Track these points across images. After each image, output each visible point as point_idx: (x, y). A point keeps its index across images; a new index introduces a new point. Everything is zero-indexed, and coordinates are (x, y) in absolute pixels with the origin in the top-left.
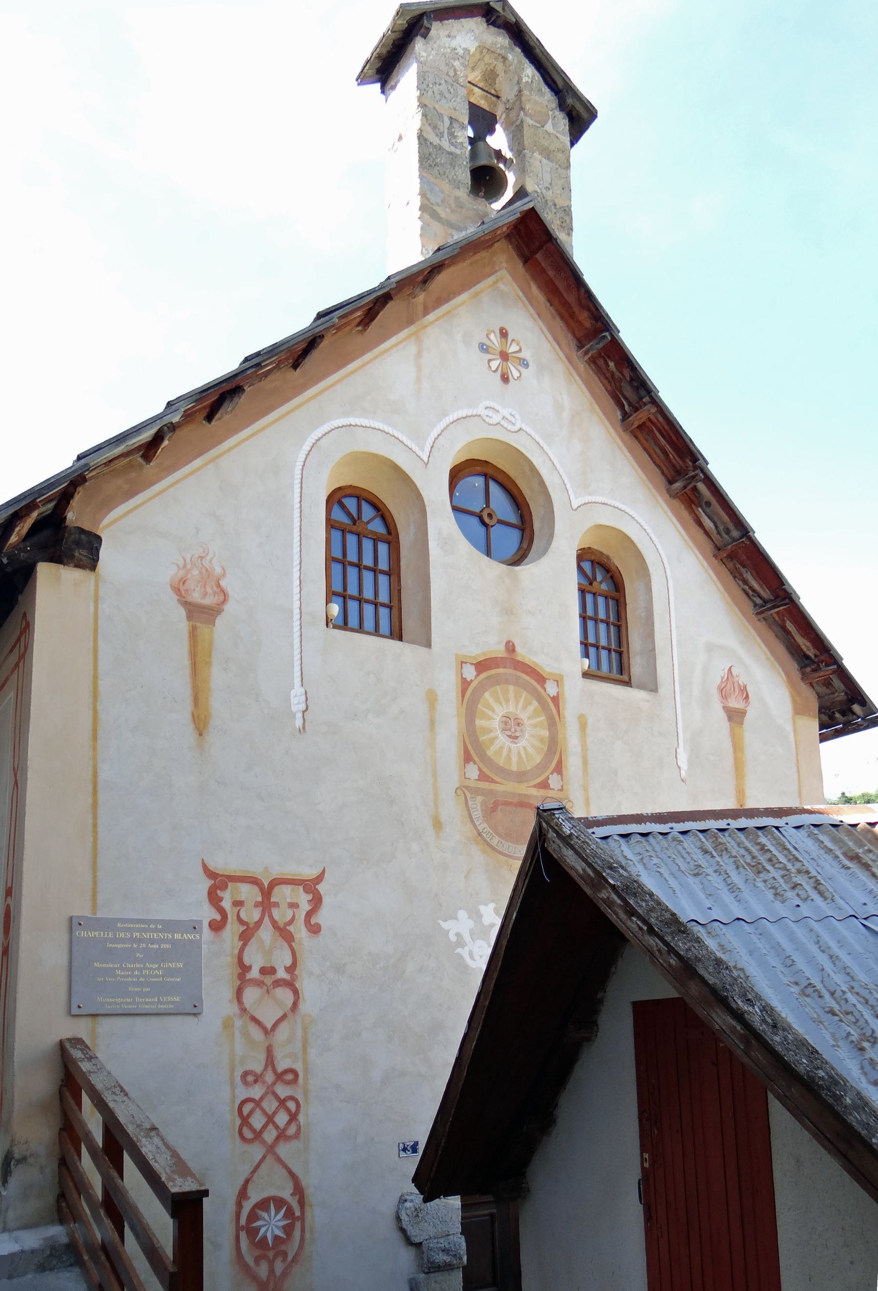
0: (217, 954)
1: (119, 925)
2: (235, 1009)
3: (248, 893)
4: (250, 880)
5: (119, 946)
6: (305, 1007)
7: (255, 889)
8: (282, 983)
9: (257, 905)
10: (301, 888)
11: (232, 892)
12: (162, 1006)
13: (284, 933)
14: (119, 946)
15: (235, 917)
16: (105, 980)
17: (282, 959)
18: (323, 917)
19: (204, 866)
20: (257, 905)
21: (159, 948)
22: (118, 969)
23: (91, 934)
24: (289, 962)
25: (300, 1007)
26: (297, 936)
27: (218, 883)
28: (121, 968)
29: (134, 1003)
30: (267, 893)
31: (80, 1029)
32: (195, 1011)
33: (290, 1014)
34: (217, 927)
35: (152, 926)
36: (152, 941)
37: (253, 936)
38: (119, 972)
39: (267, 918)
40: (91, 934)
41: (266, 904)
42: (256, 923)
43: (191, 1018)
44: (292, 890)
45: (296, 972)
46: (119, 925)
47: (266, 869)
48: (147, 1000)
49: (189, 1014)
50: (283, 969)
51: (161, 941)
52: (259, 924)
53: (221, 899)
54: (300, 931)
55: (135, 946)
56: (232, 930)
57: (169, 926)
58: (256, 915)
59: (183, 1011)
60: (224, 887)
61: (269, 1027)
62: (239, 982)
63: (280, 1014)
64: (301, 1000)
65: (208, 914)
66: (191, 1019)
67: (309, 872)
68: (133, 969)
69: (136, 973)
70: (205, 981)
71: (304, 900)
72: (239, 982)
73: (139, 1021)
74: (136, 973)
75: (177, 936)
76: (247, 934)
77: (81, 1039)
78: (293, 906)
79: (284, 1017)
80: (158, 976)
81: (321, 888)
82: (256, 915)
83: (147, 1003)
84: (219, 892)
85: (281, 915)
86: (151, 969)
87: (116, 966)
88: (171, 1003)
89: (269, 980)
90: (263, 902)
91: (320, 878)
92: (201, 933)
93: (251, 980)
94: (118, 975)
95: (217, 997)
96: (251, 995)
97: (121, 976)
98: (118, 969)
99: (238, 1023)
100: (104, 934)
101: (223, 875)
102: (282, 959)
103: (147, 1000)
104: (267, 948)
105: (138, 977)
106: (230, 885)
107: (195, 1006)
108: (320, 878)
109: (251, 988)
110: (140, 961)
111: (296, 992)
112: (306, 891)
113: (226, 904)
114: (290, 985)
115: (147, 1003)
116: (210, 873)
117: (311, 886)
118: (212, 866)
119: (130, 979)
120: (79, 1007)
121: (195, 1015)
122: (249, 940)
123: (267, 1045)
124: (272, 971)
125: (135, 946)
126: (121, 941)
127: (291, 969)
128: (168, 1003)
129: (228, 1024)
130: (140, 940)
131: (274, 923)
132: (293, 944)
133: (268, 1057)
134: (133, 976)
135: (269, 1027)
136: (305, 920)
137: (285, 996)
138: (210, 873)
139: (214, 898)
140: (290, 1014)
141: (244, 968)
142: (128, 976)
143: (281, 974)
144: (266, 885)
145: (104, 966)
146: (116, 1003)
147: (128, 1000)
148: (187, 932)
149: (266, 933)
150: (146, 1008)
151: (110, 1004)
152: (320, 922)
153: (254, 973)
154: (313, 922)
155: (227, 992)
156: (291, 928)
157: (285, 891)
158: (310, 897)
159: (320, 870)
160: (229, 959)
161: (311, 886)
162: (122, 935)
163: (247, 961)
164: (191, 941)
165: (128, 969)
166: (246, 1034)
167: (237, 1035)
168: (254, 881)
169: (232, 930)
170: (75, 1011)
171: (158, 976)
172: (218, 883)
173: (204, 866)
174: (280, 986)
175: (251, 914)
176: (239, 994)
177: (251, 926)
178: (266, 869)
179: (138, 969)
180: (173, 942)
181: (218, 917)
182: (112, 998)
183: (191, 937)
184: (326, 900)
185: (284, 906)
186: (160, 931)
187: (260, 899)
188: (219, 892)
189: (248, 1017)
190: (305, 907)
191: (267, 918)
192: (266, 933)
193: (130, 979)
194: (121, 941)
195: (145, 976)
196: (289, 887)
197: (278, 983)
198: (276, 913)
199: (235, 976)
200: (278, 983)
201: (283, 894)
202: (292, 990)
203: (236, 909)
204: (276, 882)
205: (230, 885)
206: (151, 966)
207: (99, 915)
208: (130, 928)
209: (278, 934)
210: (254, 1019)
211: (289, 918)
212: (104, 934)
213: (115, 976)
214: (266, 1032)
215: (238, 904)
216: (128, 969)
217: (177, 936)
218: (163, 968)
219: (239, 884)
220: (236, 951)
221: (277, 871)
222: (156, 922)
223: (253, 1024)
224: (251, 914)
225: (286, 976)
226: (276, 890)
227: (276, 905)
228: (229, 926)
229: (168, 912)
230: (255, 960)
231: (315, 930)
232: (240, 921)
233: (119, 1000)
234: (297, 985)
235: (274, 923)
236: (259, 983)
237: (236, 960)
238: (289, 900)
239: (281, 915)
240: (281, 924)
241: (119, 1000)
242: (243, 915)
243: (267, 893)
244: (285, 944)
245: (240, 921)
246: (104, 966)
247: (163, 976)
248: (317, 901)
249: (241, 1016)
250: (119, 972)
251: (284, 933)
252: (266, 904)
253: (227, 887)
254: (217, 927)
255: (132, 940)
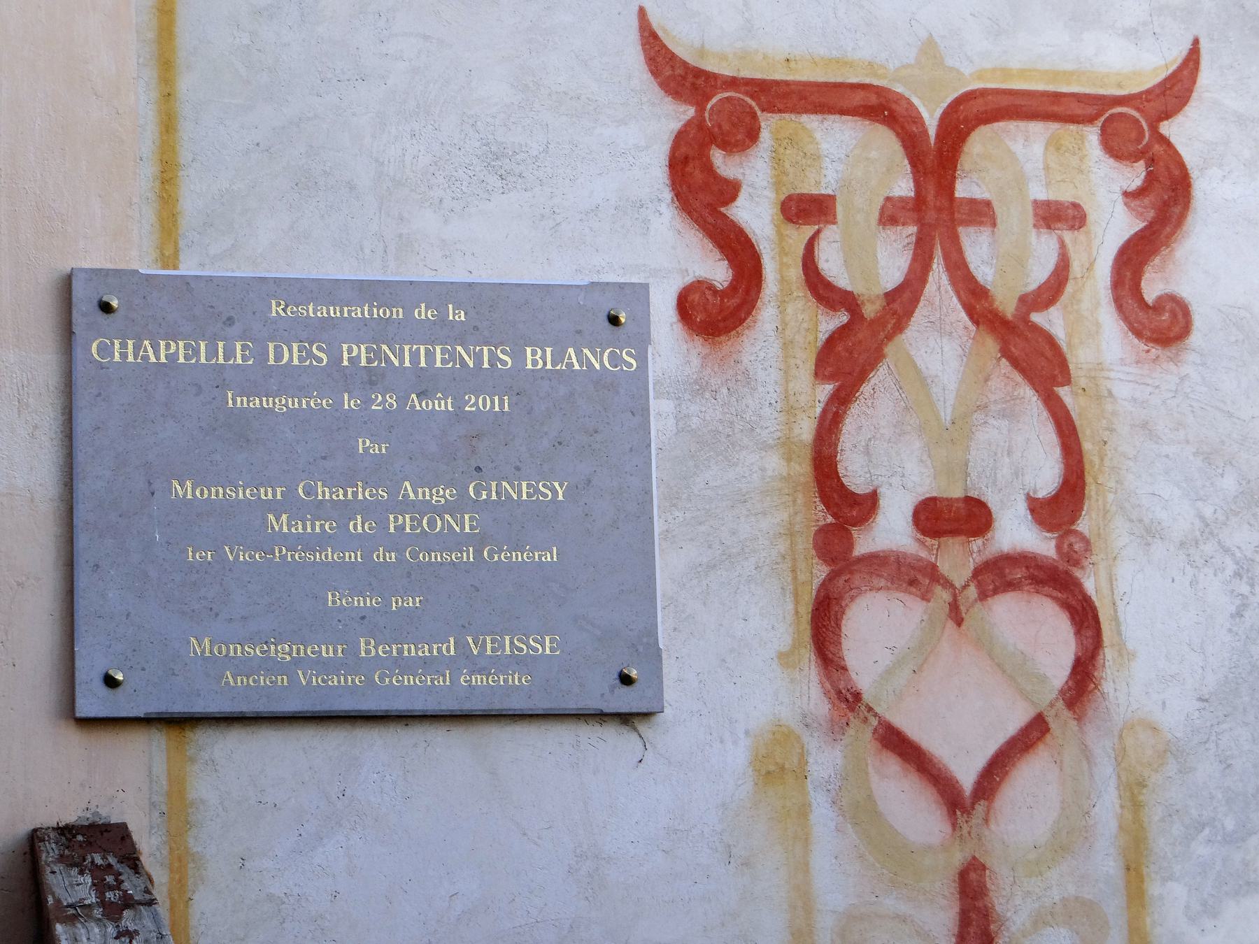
0: (717, 442)
1: (276, 309)
2: (807, 693)
3: (852, 161)
4: (858, 98)
5: (280, 404)
6: (1127, 686)
7: (883, 145)
8: (1019, 574)
9: (891, 215)
10: (1092, 135)
11: (777, 161)
12: (477, 680)
13: (1025, 346)
14: (280, 404)
15: (795, 273)
16: (220, 558)
17: (1015, 462)
18: (1196, 268)
19: (651, 40)
20: (891, 215)
21: (459, 415)
22: (275, 507)
23: (158, 353)
24: (1046, 475)
25: (1107, 687)
26: (1079, 358)
27: (715, 115)
28: (289, 506)
29: (351, 663)
30: (935, 159)
31: (118, 782)
32: (625, 700)
33: (1060, 721)
34: (714, 315)
35: (423, 313)
36: (425, 383)
37: (876, 357)
38: (281, 524)
39: (938, 276)
40: (158, 353)
41: (936, 207)
42: (891, 296)
43: (611, 734)
44: (1054, 144)
45: (1083, 526)
46: (276, 309)
47: (929, 49)
48: (410, 650)
49: (601, 717)
50: (1022, 507)
51: (462, 381)
52: (903, 301)
53: (730, 191)
54: (1091, 330)
55: (349, 403)
56: (784, 329)
57: (498, 310)
58: (889, 261)
59: (571, 705)
60: (742, 135)
61: (966, 775)
62: (821, 572)
63: (1015, 720)
64: (1109, 653)
65: (675, 257)
66: (612, 738)
67: (1125, 61)
68: (345, 510)
69: (358, 525)
70: (670, 566)
71: (1107, 194)
72: (821, 572)
73: (375, 745)
74: (358, 525)
75: (536, 358)
76: (853, 351)
77: (123, 827)
78: (1059, 216)
79: (1033, 733)
80: (458, 542)
81: (1186, 133)
82: (889, 261)
83: (404, 665)
84: (718, 157)
85: (1005, 258)
86: (422, 508)
87: (266, 494)
88: (520, 662)
89: (957, 560)
90: (918, 204)
91: (1176, 89)
92: (642, 343)
93: (877, 561)
94: (284, 539)
95: (727, 641)
96: (878, 628)
97: (292, 542)
98: (275, 507)
99: (825, 760)
100: (212, 352)
101: (733, 83)
102: (1015, 462)
103: (410, 650)
104: (946, 414)
105: (365, 543)
106: (769, 124)
107: (626, 680)
108: (1176, 89)
109: (880, 597)
110: (376, 471)
111: (1084, 617)
112: (1114, 148)
113: (755, 213)
114: (1059, 581)
115: (404, 665)
116: (675, 74)
117: (1138, 126)
118: (684, 39)
119: (330, 555)
120: (110, 682)
121: (626, 719)
122: (862, 377)
123: (958, 858)
124: (972, 517)
125: (349, 403)
126: (289, 380)
127: (1061, 508)
128: (500, 664)
129: (777, 766)
130: (373, 379)
131: (974, 297)
132: (1064, 392)
133: (965, 920)
134: (343, 540)
135: (966, 775)
136: (1117, 284)
137: (1033, 631)
138: (675, 74)
139: (697, 187)
140: (1060, 721)
141: (845, 507)
142: (321, 542)
143: (1016, 532)
144: (931, 120)
145: (216, 493)
146: (270, 666)
147: (326, 652)
148: (579, 338)
149: (938, 345)
150: (408, 690)
151: (245, 667)
152: (1184, 291)
153: (892, 530)
154: (1151, 291)
155: (768, 618)
156: (1052, 320)
157: (1017, 147)
158: (1135, 175)
159: (1175, 54)
160: (774, 463)
161: (1138, 126)
162: (292, 355)
163: (855, 472)
164: (602, 383)
165: (319, 509)
166: (862, 814)
167: (822, 814)
168: (878, 106)
169: (784, 329)
170: (92, 702)
171: (455, 542)
172: (715, 115)
173: (651, 40)
174: (1010, 586)
175: (870, 259)
176: (824, 624)
177: (870, 311)
178: (929, 49)
179: (367, 509)
180: (518, 386)
181: (719, 273)
182: (252, 641)
183: (600, 361)
184: (1205, 187)
185: (1014, 217)
186: (461, 335)
187: (904, 187)
188: (718, 157)
189: (868, 734)
190: (1113, 224)
191: (938, 276)
192: (938, 345)
193: (330, 555)
194: (289, 380)
195: (397, 542)
196: (1038, 130)
197: (1000, 574)
198: (979, 249)
199: (805, 544)
200: (1000, 574)
201: (1011, 165)
202: (1066, 606)
203: (799, 236)
204: (975, 111)
205: (769, 124)
206: (424, 494)
207: (188, 267)
208: (327, 323)
209: (991, 345)
210: (896, 743)
211: (1039, 273)
212: (212, 352)
213: (266, 543)
214: (954, 802)
215: (807, 209)
216: (319, 509)
217: (533, 358)
218: (477, 506)
219: (811, 121)
220: (806, 430)
221: (979, 60)
222: (440, 293)
223: (893, 764)
224: (870, 259)
225: (1041, 544)
226: (979, 144)
227: (981, 213)
228: (767, 314)
229: (492, 245)
230: (894, 467)
231: (1162, 326)
232: (819, 287)
233: (282, 652)
234: (1089, 585)
235: (974, 297)
236: (912, 576)
237: (803, 469)
238: (1039, 192)
239: (1005, 258)
240: (1007, 304)
241: (282, 652)
242: (831, 264)
243: (935, 159)
244: (1027, 393)
245: (819, 287)
246: (216, 493)
247: (479, 541)
248: (1167, 196)
249: (836, 729)
250: (281, 524)
251: (1025, 346)
252: (936, 207)
253: (753, 135)
254: (714, 315)
255: (340, 377)
